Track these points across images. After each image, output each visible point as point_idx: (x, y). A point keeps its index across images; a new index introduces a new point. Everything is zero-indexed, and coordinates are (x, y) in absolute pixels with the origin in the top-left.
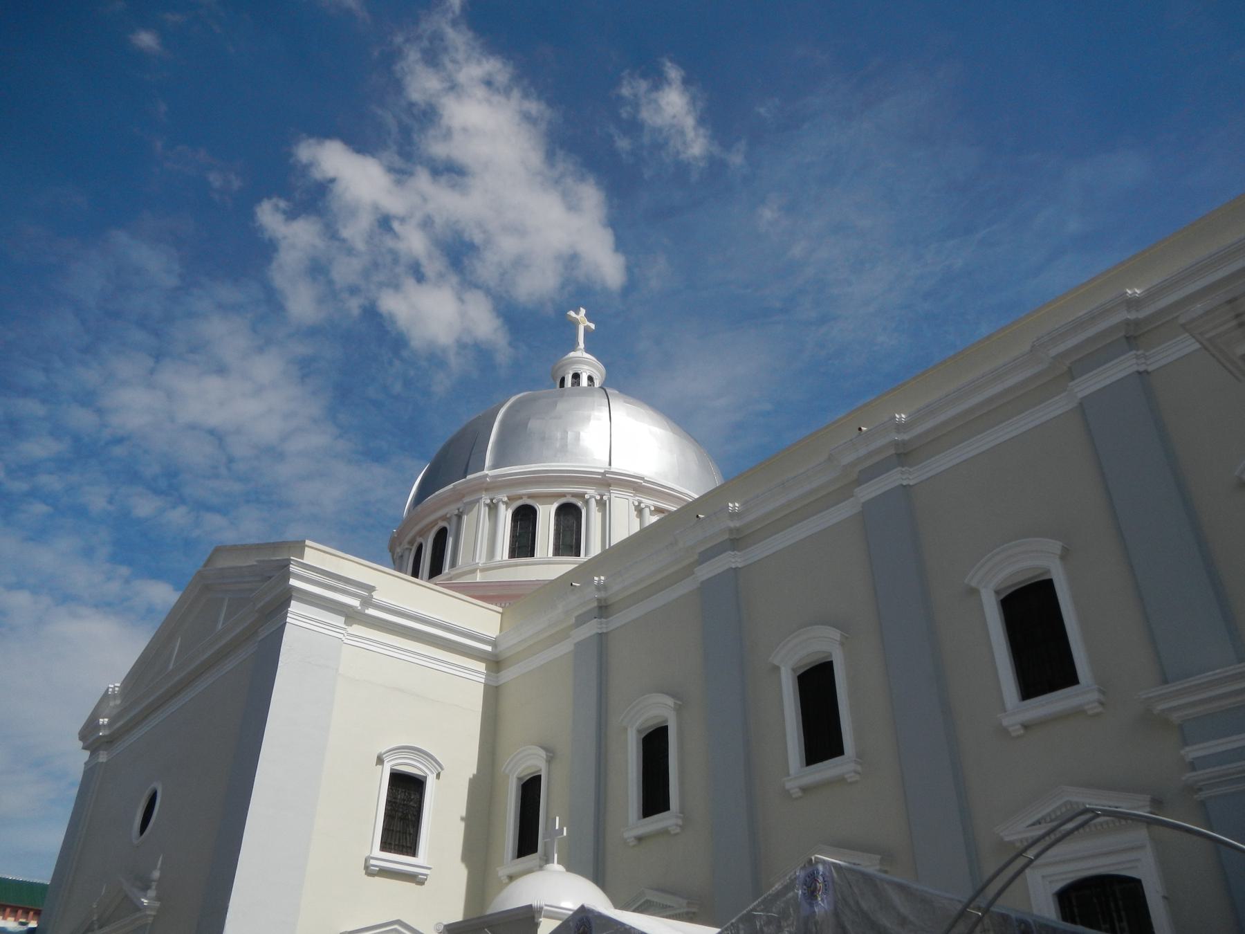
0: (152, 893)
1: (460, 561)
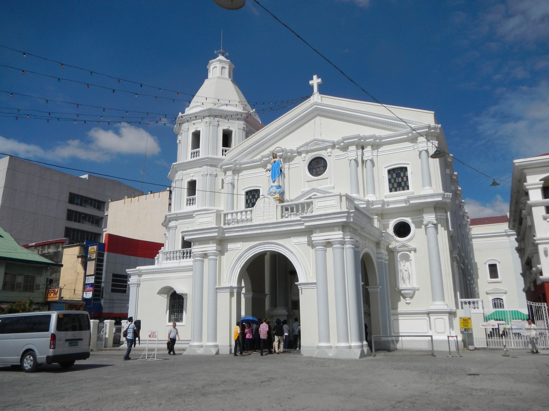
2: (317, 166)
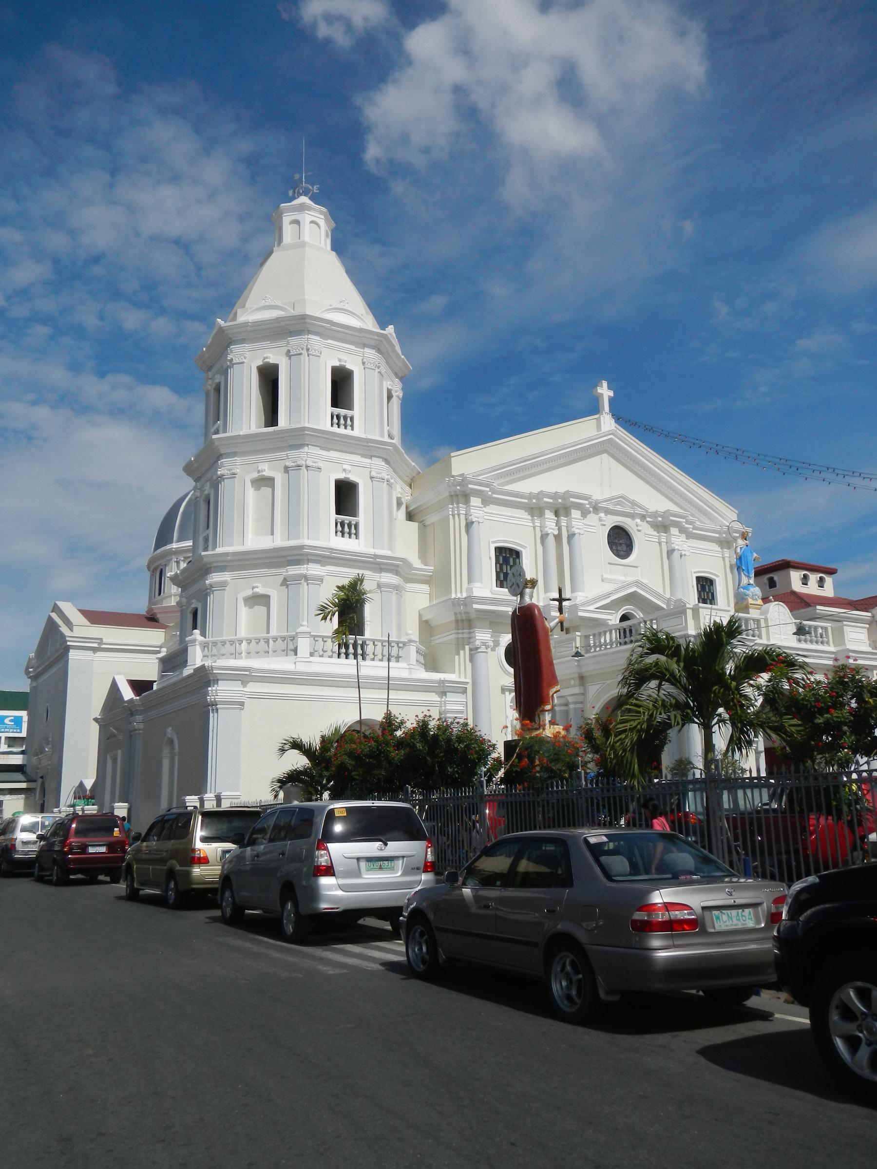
0: (50, 746)
1: (166, 591)
2: (619, 540)
